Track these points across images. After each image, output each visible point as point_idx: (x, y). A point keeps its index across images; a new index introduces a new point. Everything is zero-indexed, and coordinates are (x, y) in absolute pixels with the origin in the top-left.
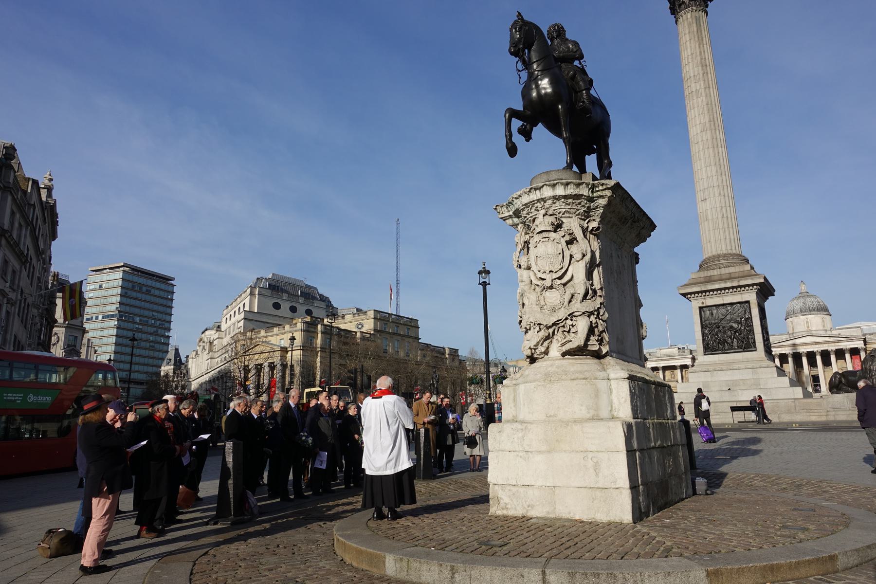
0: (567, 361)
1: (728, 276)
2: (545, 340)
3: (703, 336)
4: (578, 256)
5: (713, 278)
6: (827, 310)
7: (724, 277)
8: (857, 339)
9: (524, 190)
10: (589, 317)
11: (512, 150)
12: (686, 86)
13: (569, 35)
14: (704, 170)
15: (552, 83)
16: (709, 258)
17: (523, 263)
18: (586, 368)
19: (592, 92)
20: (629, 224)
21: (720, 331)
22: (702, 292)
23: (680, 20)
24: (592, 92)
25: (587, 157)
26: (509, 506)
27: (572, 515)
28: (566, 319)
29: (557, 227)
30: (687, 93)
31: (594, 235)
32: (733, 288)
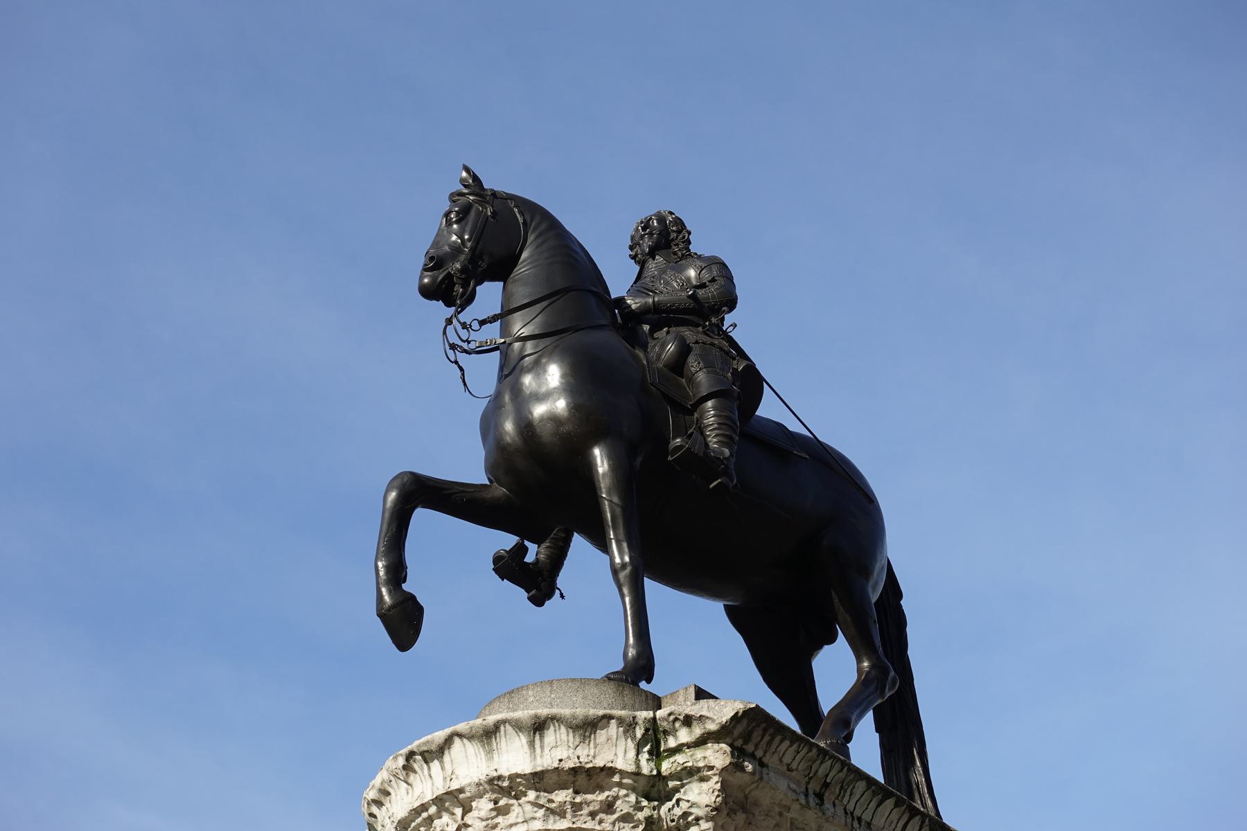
9: (390, 763)
11: (403, 621)
15: (576, 384)
19: (768, 409)
24: (768, 409)
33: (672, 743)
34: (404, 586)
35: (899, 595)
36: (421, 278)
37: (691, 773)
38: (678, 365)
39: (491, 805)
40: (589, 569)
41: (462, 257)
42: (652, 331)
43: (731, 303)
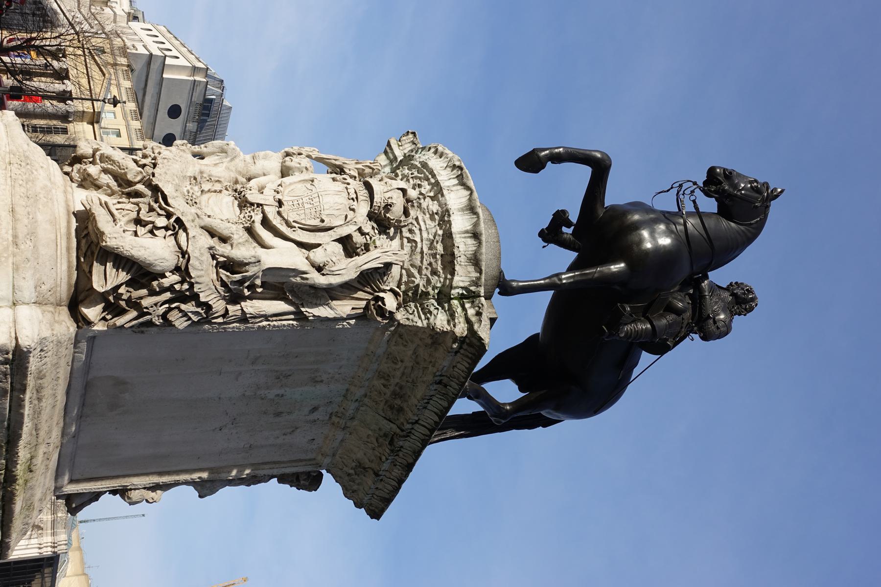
0: (64, 224)
2: (116, 177)
4: (318, 255)
9: (457, 157)
10: (177, 269)
11: (531, 163)
13: (738, 321)
17: (293, 162)
18: (46, 252)
19: (646, 358)
20: (388, 426)
24: (646, 358)
28: (169, 215)
29: (381, 221)
31: (367, 308)
33: (467, 306)
34: (549, 163)
35: (544, 426)
36: (719, 168)
37: (452, 315)
38: (671, 309)
39: (435, 211)
40: (559, 261)
41: (731, 190)
42: (689, 295)
43: (705, 338)
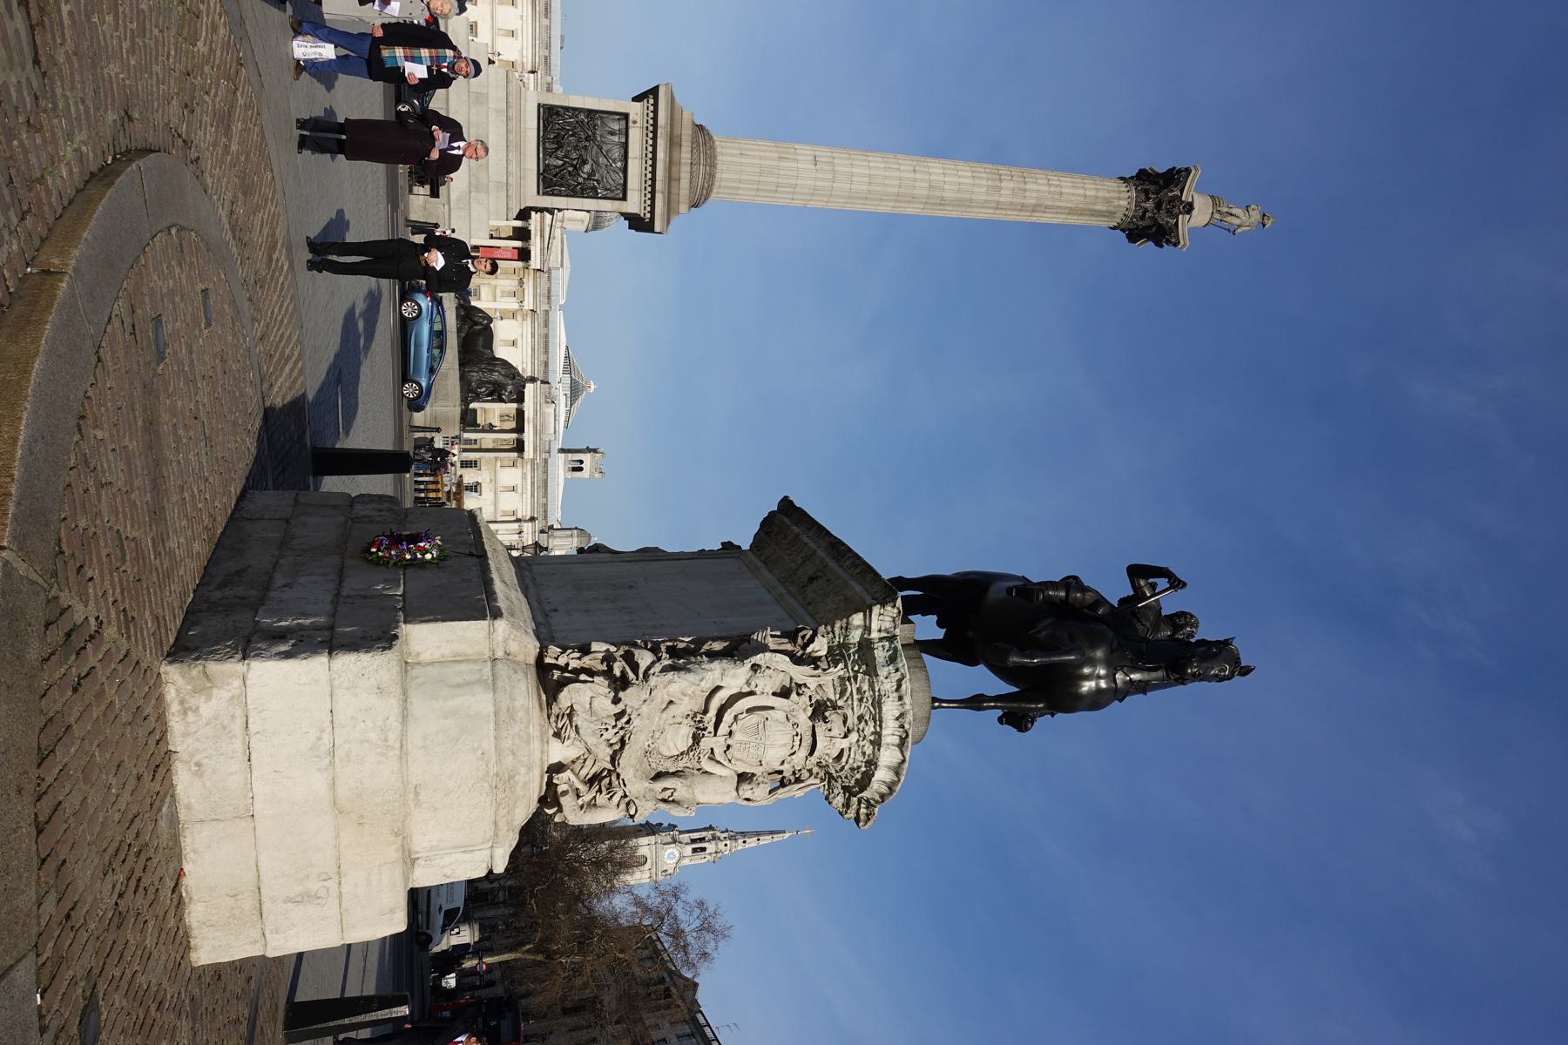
1: (675, 175)
3: (575, 109)
5: (676, 149)
6: (595, 228)
7: (674, 169)
8: (543, 262)
12: (1015, 171)
14: (867, 171)
16: (713, 148)
21: (579, 140)
22: (655, 125)
23: (1123, 187)
25: (934, 618)
26: (191, 717)
27: (192, 855)
30: (1003, 171)
32: (653, 179)
